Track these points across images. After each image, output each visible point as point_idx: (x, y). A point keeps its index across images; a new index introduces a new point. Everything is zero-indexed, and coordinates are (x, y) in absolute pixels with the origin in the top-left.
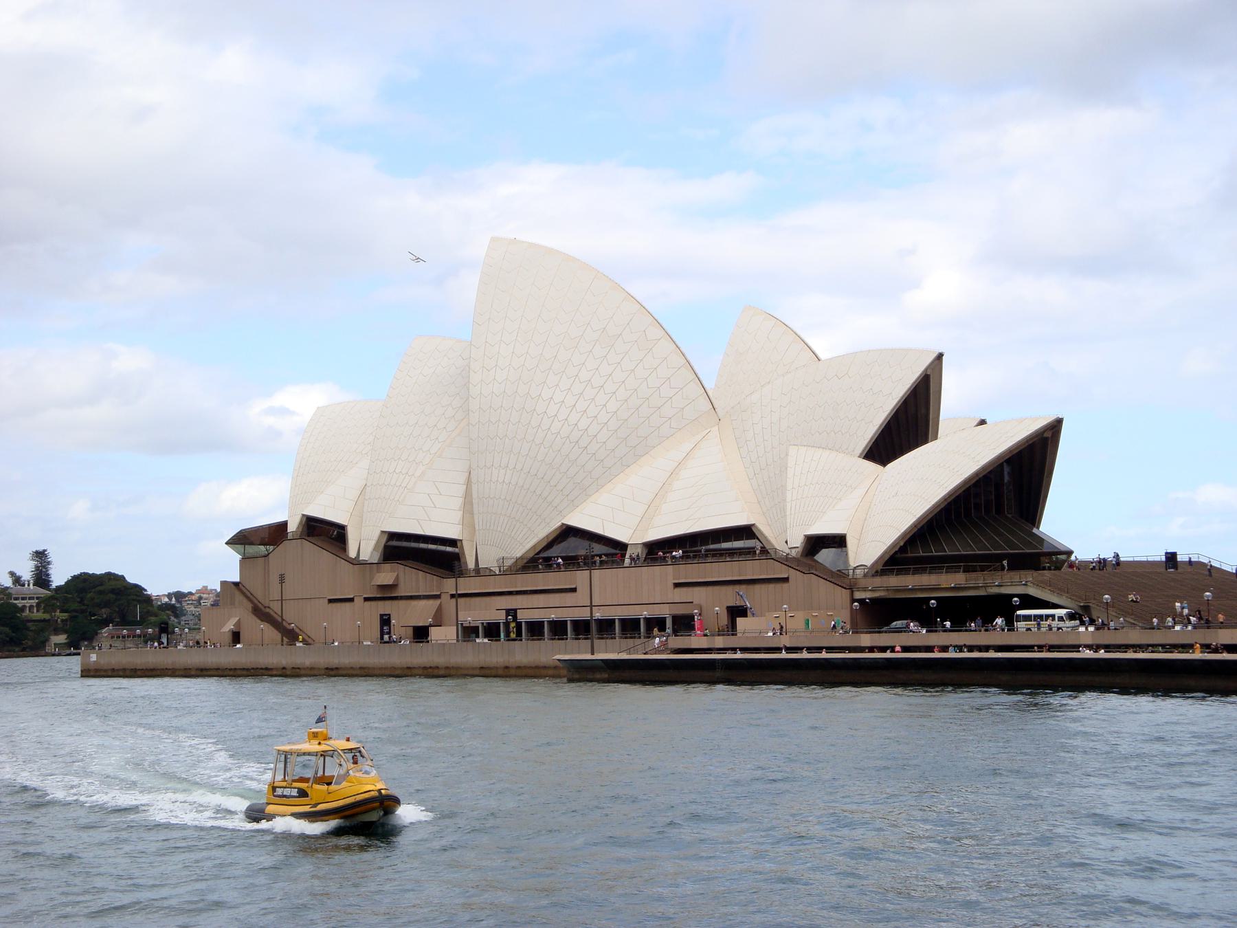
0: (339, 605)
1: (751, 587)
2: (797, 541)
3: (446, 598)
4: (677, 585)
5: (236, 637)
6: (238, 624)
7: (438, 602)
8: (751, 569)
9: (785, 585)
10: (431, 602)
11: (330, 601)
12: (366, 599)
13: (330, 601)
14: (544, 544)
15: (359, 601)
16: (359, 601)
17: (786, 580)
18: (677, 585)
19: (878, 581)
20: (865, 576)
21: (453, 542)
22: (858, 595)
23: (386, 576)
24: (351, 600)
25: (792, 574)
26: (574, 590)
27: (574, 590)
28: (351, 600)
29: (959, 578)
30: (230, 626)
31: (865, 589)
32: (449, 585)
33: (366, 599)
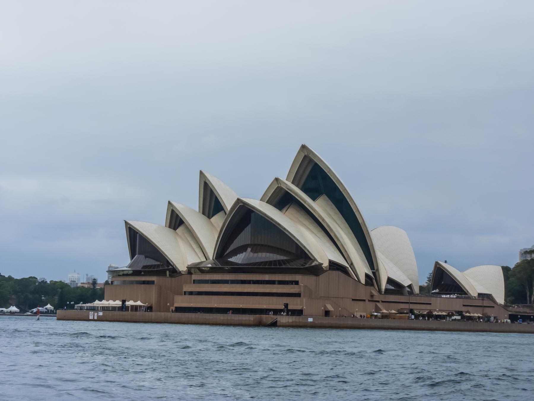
0: (357, 302)
2: (476, 295)
3: (380, 302)
4: (464, 305)
5: (327, 313)
9: (493, 309)
11: (353, 300)
12: (369, 301)
13: (353, 300)
15: (367, 301)
16: (367, 301)
17: (493, 307)
26: (430, 304)
27: (430, 304)
30: (330, 308)
31: (510, 311)
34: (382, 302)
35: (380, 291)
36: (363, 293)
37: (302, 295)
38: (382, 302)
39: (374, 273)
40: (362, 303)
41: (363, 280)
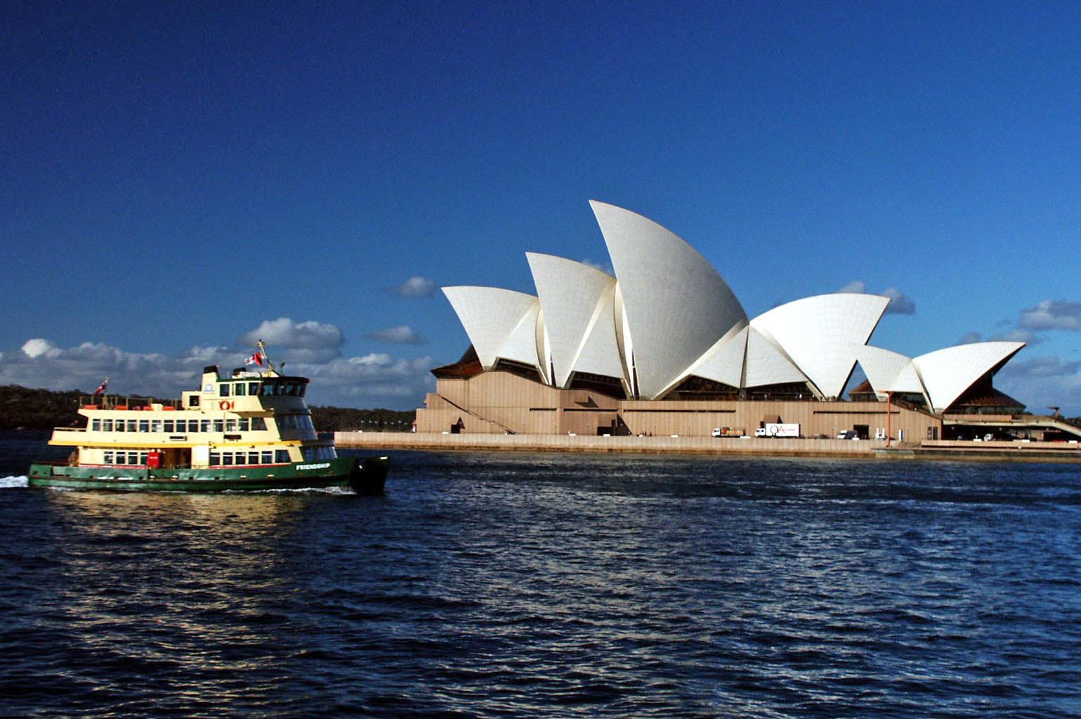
0: (541, 412)
1: (871, 416)
5: (456, 429)
6: (460, 420)
7: (615, 413)
8: (871, 406)
9: (897, 416)
10: (610, 413)
11: (531, 410)
12: (565, 410)
13: (531, 410)
14: (678, 384)
15: (558, 410)
17: (898, 413)
18: (814, 413)
19: (955, 416)
20: (943, 413)
21: (618, 380)
22: (945, 423)
23: (583, 395)
24: (555, 409)
25: (902, 410)
26: (734, 411)
27: (734, 411)
28: (555, 409)
29: (1009, 417)
31: (950, 420)
32: (625, 404)
33: (565, 410)
34: (625, 411)
35: (637, 397)
36: (551, 398)
37: (428, 405)
38: (625, 411)
39: (634, 370)
40: (550, 412)
41: (562, 381)
